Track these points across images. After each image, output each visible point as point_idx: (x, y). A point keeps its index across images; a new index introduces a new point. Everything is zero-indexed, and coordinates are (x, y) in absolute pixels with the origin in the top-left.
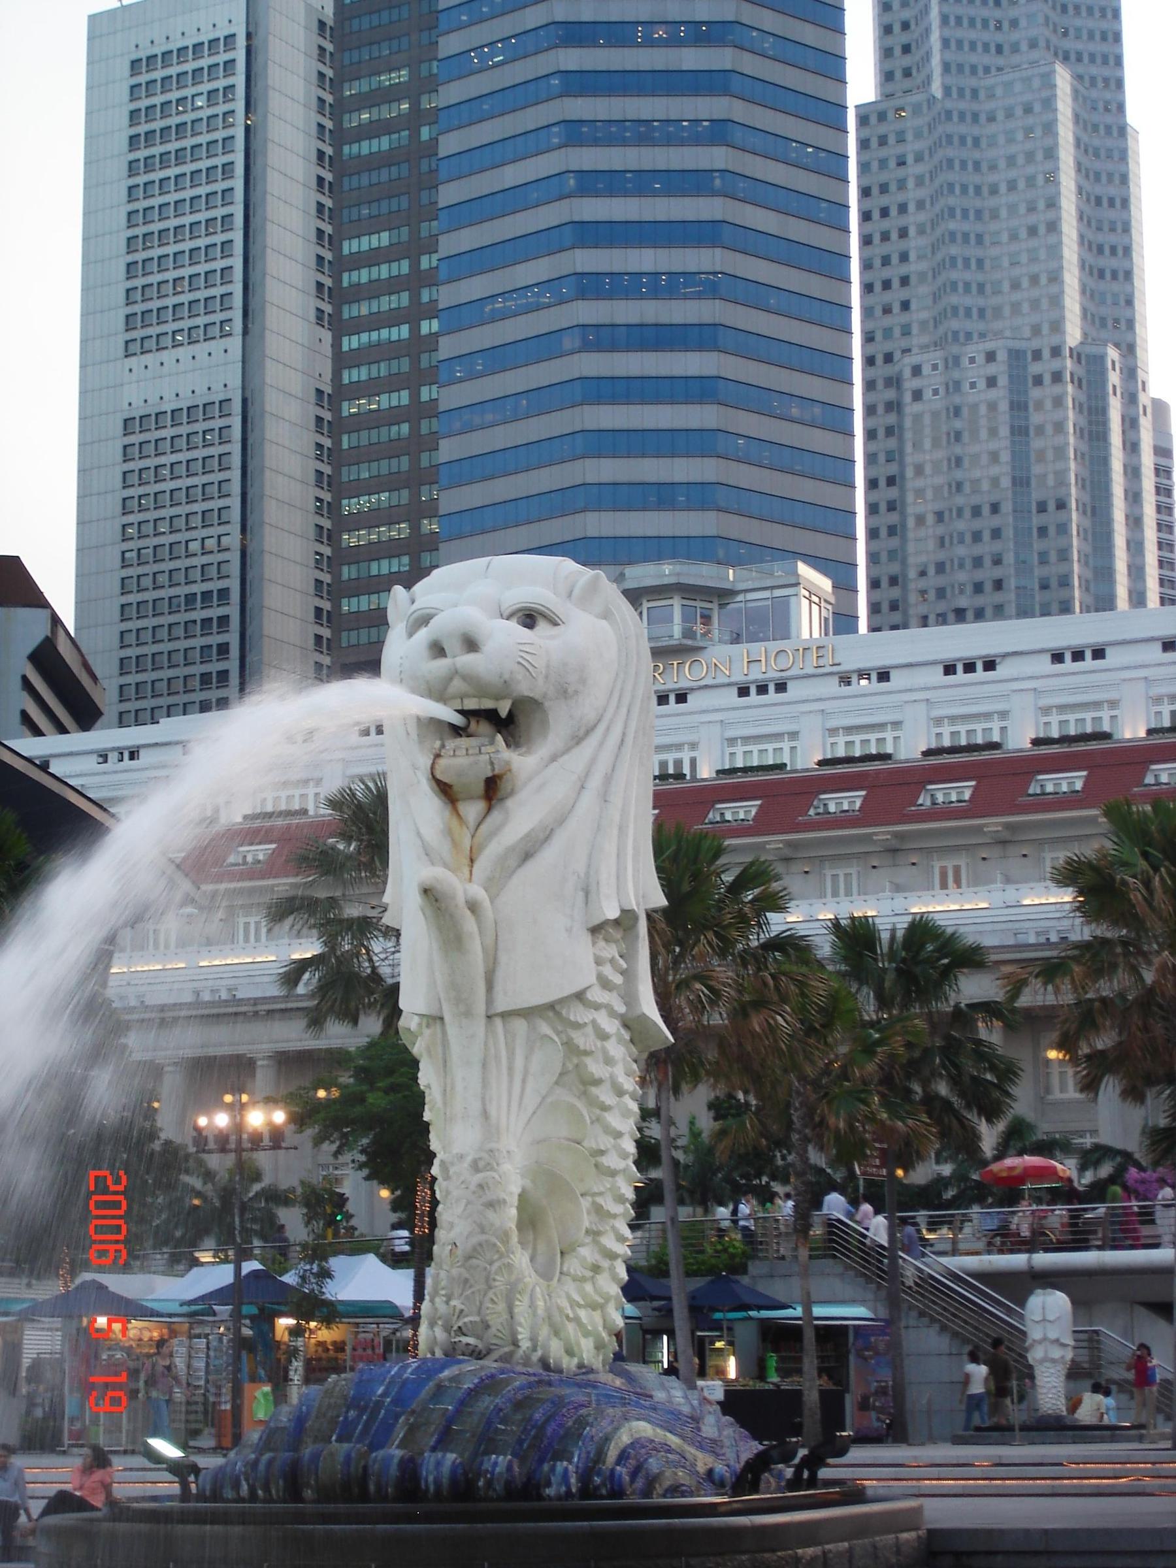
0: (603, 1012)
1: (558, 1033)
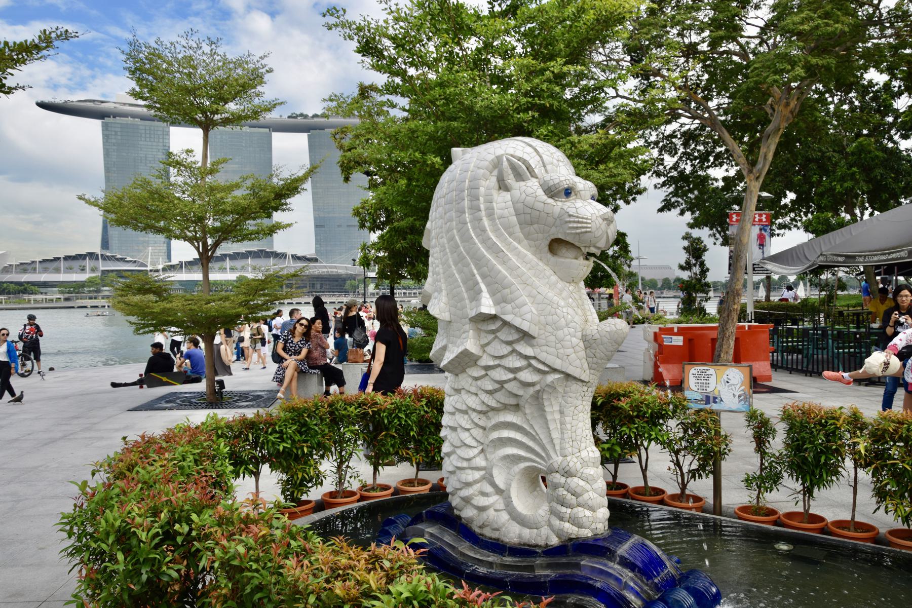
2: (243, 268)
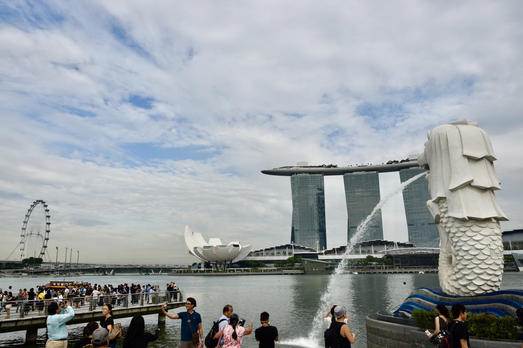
2: (369, 252)
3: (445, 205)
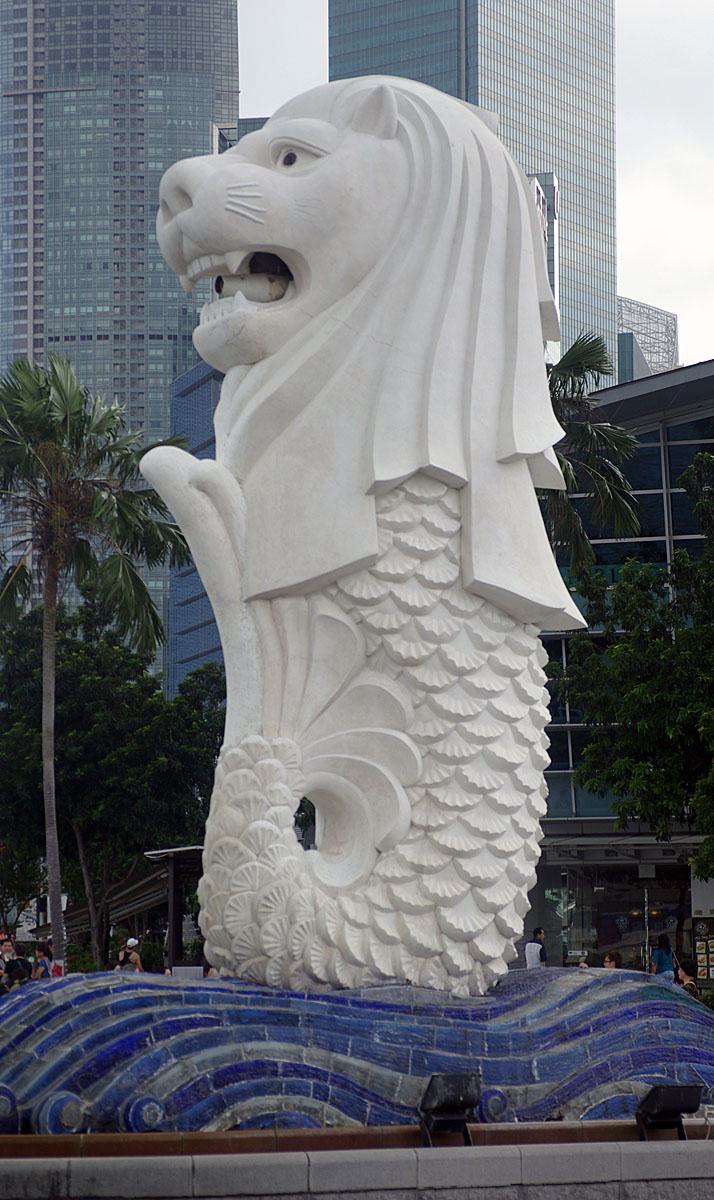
0: (414, 582)
1: (348, 612)
3: (433, 515)
